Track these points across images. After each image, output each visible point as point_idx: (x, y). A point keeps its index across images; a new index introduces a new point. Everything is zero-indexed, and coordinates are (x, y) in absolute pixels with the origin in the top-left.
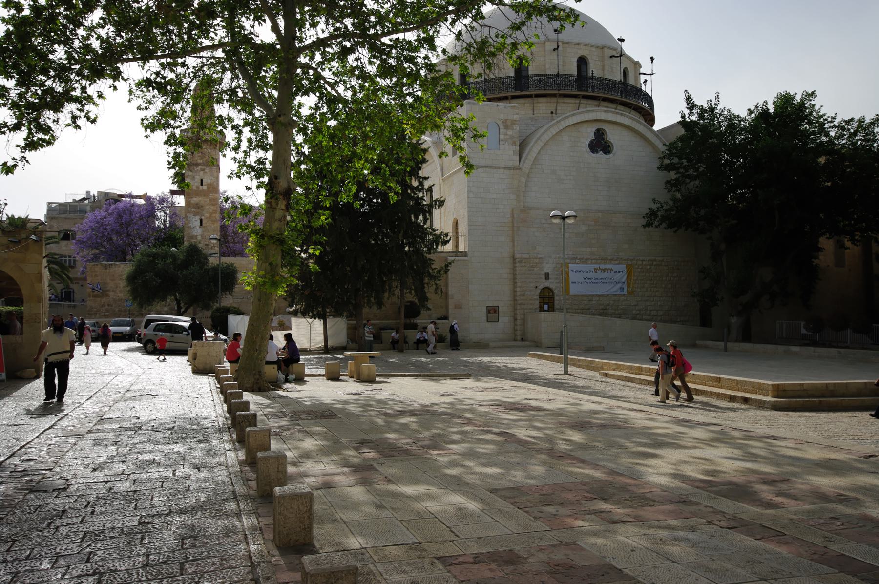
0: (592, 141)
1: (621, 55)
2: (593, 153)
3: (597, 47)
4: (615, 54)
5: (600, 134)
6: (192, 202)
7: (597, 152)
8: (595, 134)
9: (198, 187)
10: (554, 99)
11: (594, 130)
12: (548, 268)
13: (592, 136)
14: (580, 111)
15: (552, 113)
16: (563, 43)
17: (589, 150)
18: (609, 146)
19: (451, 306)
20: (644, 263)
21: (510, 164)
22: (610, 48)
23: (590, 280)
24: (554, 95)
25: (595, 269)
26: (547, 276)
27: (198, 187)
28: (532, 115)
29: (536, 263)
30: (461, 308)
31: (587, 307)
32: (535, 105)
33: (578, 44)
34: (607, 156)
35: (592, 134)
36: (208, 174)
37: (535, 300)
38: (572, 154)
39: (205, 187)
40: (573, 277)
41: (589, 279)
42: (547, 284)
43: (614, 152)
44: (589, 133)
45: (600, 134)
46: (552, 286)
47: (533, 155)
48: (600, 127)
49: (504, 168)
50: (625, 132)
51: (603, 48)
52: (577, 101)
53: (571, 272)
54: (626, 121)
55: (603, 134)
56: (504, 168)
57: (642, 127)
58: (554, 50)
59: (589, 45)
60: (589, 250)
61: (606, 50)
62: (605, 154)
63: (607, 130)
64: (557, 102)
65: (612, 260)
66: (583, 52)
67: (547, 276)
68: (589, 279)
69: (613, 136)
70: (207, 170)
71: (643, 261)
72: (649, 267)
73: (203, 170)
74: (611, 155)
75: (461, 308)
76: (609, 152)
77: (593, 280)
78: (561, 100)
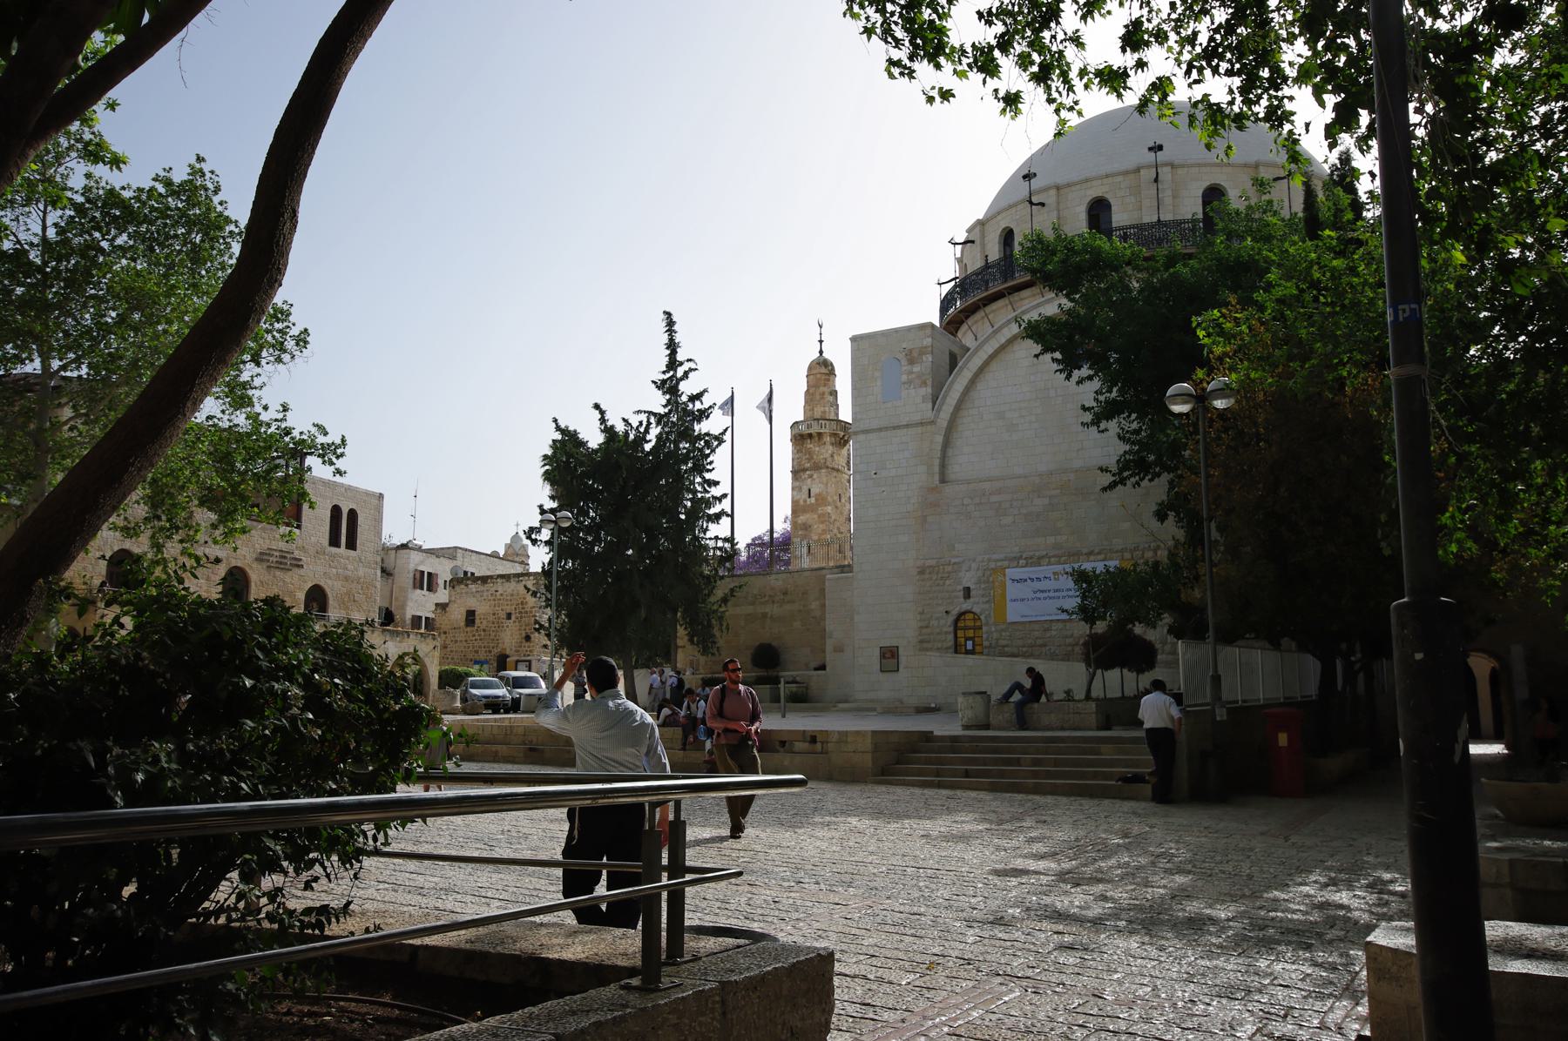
6: (800, 522)
9: (805, 501)
12: (968, 579)
19: (829, 648)
21: (917, 418)
23: (1046, 595)
25: (1054, 573)
26: (967, 593)
27: (805, 501)
29: (949, 573)
30: (842, 651)
31: (1039, 642)
36: (817, 481)
37: (946, 633)
38: (1032, 378)
39: (813, 500)
40: (1012, 590)
41: (1042, 591)
49: (907, 426)
53: (1009, 583)
56: (907, 426)
60: (1051, 540)
65: (1090, 553)
67: (967, 593)
68: (1042, 591)
70: (815, 476)
73: (811, 476)
75: (842, 651)
77: (1051, 594)
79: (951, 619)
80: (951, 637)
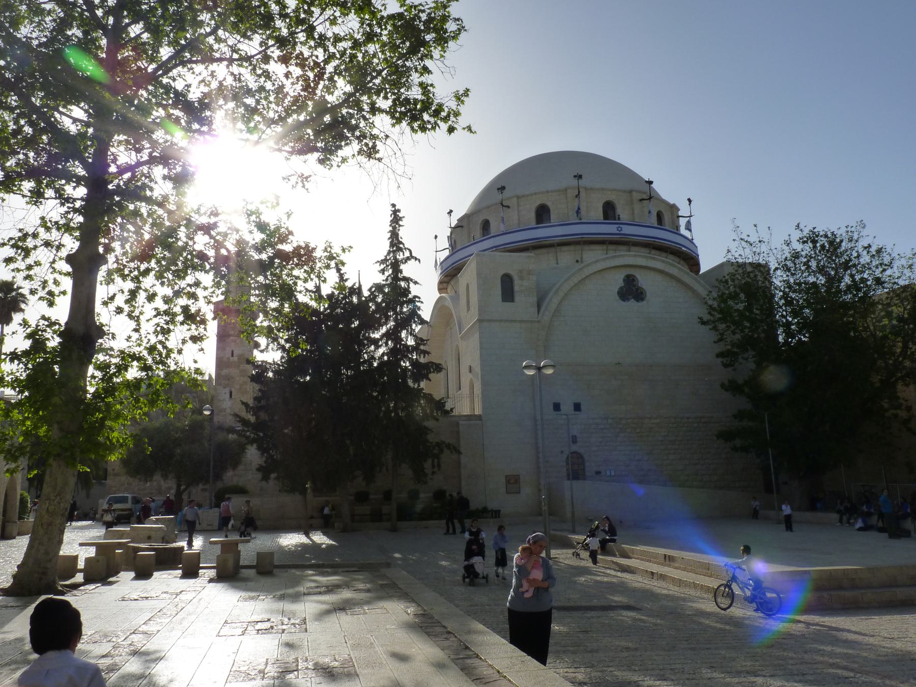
0: (621, 288)
1: (650, 198)
2: (624, 300)
3: (624, 191)
4: (645, 197)
5: (630, 280)
7: (628, 300)
8: (624, 280)
10: (578, 247)
11: (623, 276)
13: (621, 283)
14: (608, 256)
15: (577, 261)
16: (586, 189)
17: (618, 298)
18: (642, 293)
20: (690, 420)
22: (639, 192)
28: (555, 265)
32: (558, 254)
33: (603, 189)
34: (640, 304)
42: (574, 448)
43: (647, 298)
44: (617, 280)
45: (630, 280)
46: (581, 451)
47: (553, 306)
50: (659, 278)
51: (631, 192)
52: (605, 247)
54: (658, 265)
55: (633, 280)
57: (677, 270)
58: (576, 197)
59: (614, 190)
61: (634, 193)
62: (637, 301)
63: (638, 276)
64: (582, 250)
69: (645, 281)
71: (688, 418)
72: (696, 425)
74: (645, 302)
76: (642, 299)
78: (586, 247)
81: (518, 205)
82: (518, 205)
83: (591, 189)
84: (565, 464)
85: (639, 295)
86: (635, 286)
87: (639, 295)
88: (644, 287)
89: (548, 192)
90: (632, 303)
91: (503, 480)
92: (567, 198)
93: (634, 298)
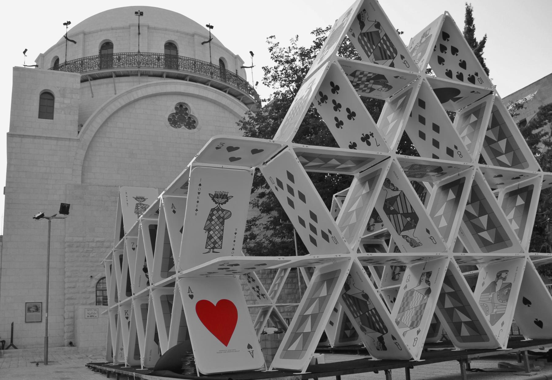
5: (182, 108)
8: (176, 108)
18: (194, 122)
24: (135, 74)
32: (117, 85)
33: (166, 30)
35: (173, 107)
43: (198, 127)
45: (182, 108)
48: (182, 101)
50: (212, 108)
55: (186, 109)
59: (177, 32)
62: (190, 128)
63: (190, 105)
66: (172, 37)
74: (195, 130)
76: (194, 127)
79: (94, 282)
80: (94, 296)
81: (84, 41)
82: (84, 41)
83: (155, 28)
84: (94, 290)
85: (191, 124)
86: (187, 114)
87: (191, 124)
88: (196, 116)
89: (112, 29)
90: (183, 130)
91: (23, 308)
92: (130, 36)
93: (185, 125)
